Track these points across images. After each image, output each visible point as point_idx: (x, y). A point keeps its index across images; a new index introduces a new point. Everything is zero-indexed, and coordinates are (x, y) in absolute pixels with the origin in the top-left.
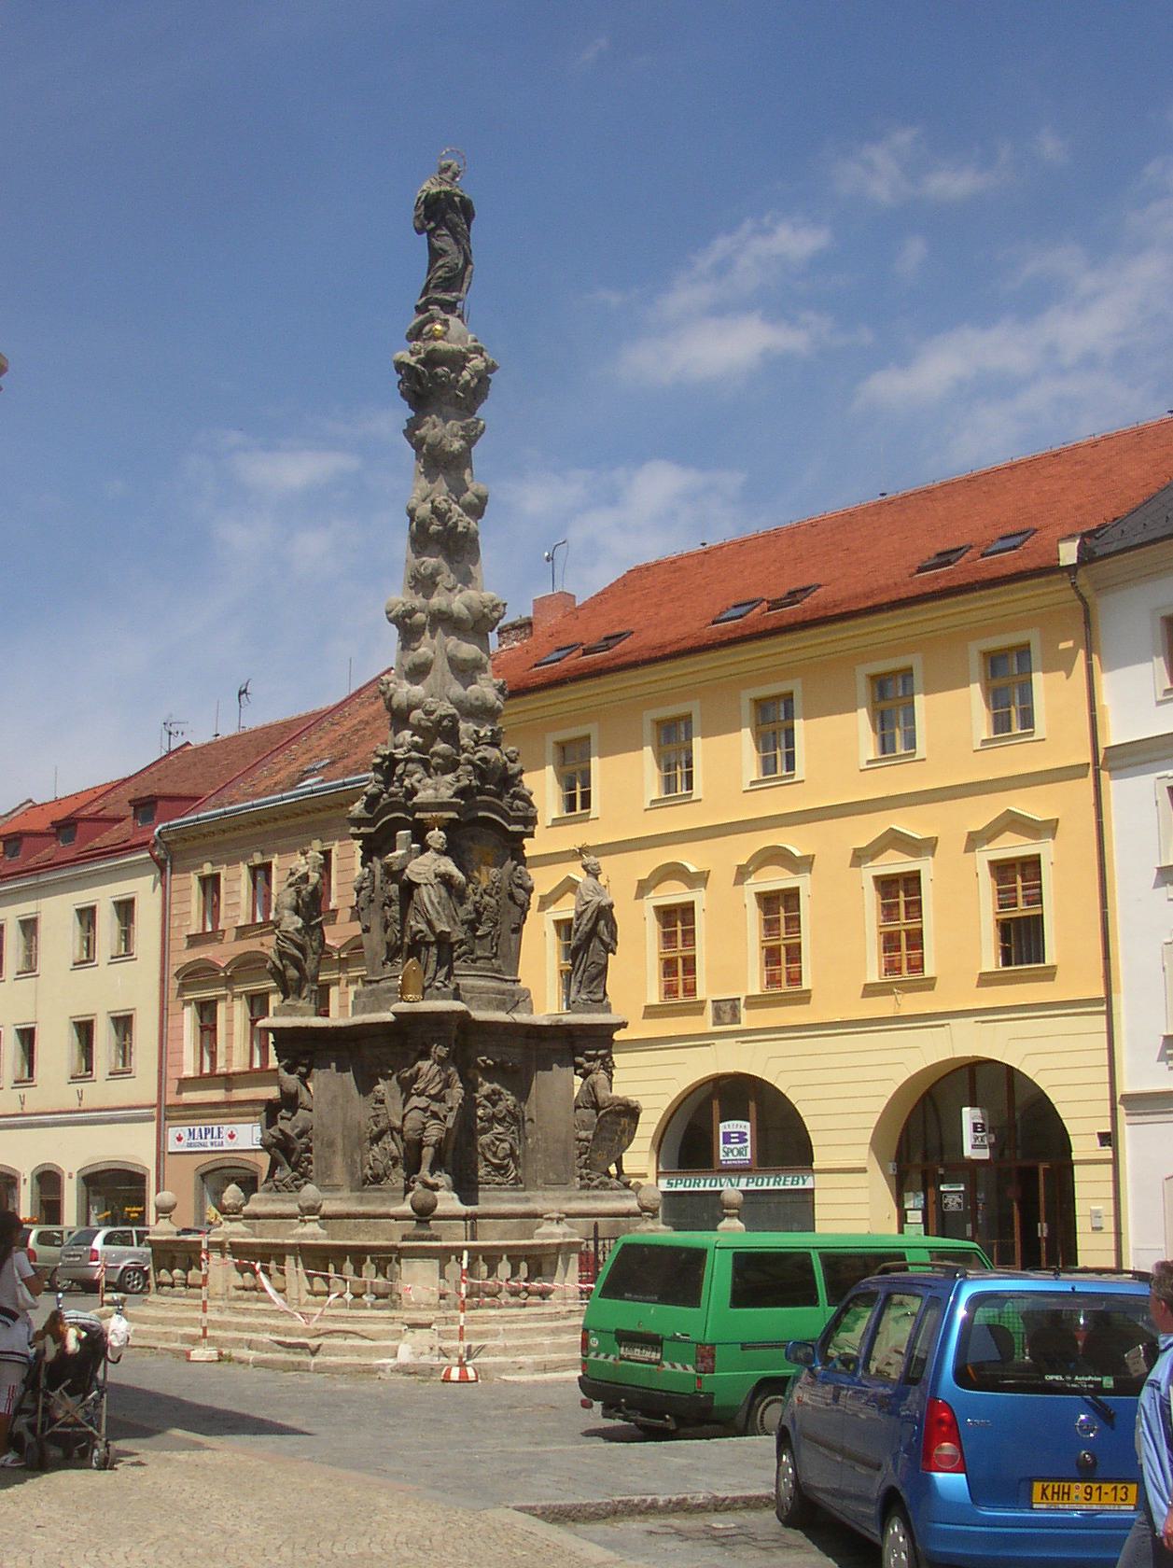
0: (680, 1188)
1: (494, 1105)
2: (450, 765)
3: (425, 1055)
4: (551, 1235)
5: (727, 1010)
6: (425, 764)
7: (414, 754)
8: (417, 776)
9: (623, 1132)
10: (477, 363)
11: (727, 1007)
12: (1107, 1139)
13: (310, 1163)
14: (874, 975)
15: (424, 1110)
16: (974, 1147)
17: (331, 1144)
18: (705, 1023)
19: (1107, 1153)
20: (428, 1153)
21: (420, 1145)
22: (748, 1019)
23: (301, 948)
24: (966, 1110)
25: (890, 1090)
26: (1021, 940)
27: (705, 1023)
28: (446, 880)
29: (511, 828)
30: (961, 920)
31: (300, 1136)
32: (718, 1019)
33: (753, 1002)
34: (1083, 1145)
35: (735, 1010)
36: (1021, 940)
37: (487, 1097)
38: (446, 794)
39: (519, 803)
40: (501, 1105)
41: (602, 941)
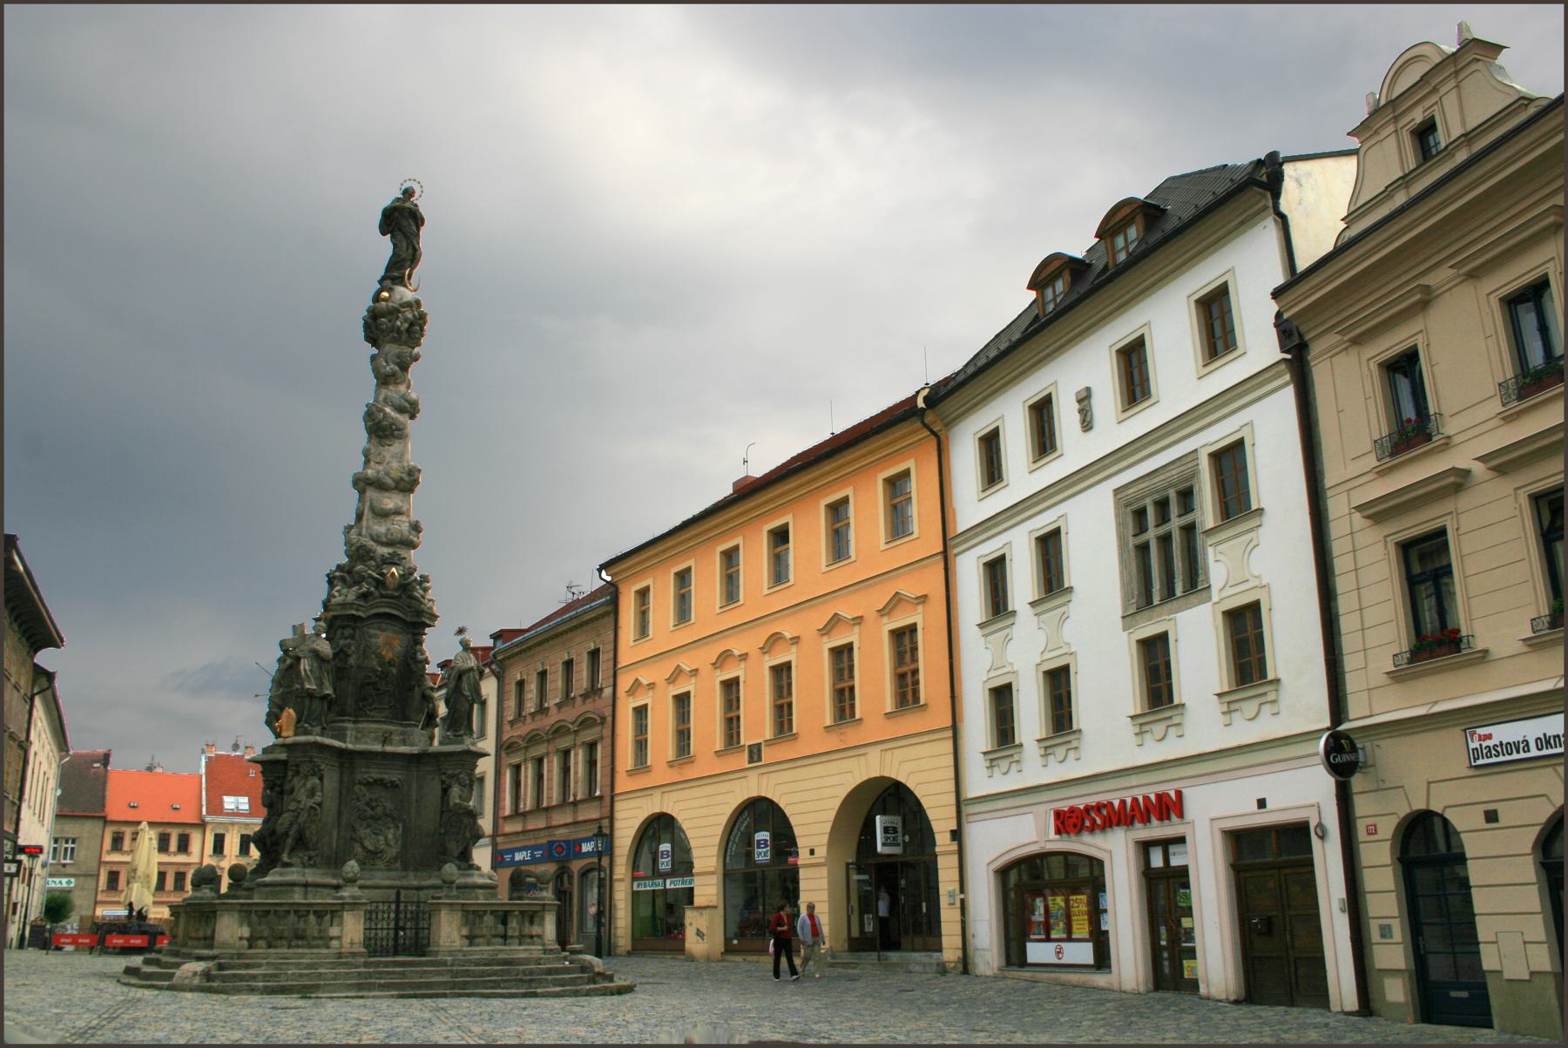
3: (298, 773)
5: (755, 753)
6: (343, 579)
12: (957, 835)
14: (828, 722)
20: (290, 841)
21: (286, 834)
22: (767, 755)
25: (836, 803)
27: (743, 760)
29: (409, 619)
32: (751, 760)
33: (769, 743)
34: (943, 841)
35: (759, 751)
36: (907, 691)
37: (368, 804)
38: (351, 597)
40: (379, 810)
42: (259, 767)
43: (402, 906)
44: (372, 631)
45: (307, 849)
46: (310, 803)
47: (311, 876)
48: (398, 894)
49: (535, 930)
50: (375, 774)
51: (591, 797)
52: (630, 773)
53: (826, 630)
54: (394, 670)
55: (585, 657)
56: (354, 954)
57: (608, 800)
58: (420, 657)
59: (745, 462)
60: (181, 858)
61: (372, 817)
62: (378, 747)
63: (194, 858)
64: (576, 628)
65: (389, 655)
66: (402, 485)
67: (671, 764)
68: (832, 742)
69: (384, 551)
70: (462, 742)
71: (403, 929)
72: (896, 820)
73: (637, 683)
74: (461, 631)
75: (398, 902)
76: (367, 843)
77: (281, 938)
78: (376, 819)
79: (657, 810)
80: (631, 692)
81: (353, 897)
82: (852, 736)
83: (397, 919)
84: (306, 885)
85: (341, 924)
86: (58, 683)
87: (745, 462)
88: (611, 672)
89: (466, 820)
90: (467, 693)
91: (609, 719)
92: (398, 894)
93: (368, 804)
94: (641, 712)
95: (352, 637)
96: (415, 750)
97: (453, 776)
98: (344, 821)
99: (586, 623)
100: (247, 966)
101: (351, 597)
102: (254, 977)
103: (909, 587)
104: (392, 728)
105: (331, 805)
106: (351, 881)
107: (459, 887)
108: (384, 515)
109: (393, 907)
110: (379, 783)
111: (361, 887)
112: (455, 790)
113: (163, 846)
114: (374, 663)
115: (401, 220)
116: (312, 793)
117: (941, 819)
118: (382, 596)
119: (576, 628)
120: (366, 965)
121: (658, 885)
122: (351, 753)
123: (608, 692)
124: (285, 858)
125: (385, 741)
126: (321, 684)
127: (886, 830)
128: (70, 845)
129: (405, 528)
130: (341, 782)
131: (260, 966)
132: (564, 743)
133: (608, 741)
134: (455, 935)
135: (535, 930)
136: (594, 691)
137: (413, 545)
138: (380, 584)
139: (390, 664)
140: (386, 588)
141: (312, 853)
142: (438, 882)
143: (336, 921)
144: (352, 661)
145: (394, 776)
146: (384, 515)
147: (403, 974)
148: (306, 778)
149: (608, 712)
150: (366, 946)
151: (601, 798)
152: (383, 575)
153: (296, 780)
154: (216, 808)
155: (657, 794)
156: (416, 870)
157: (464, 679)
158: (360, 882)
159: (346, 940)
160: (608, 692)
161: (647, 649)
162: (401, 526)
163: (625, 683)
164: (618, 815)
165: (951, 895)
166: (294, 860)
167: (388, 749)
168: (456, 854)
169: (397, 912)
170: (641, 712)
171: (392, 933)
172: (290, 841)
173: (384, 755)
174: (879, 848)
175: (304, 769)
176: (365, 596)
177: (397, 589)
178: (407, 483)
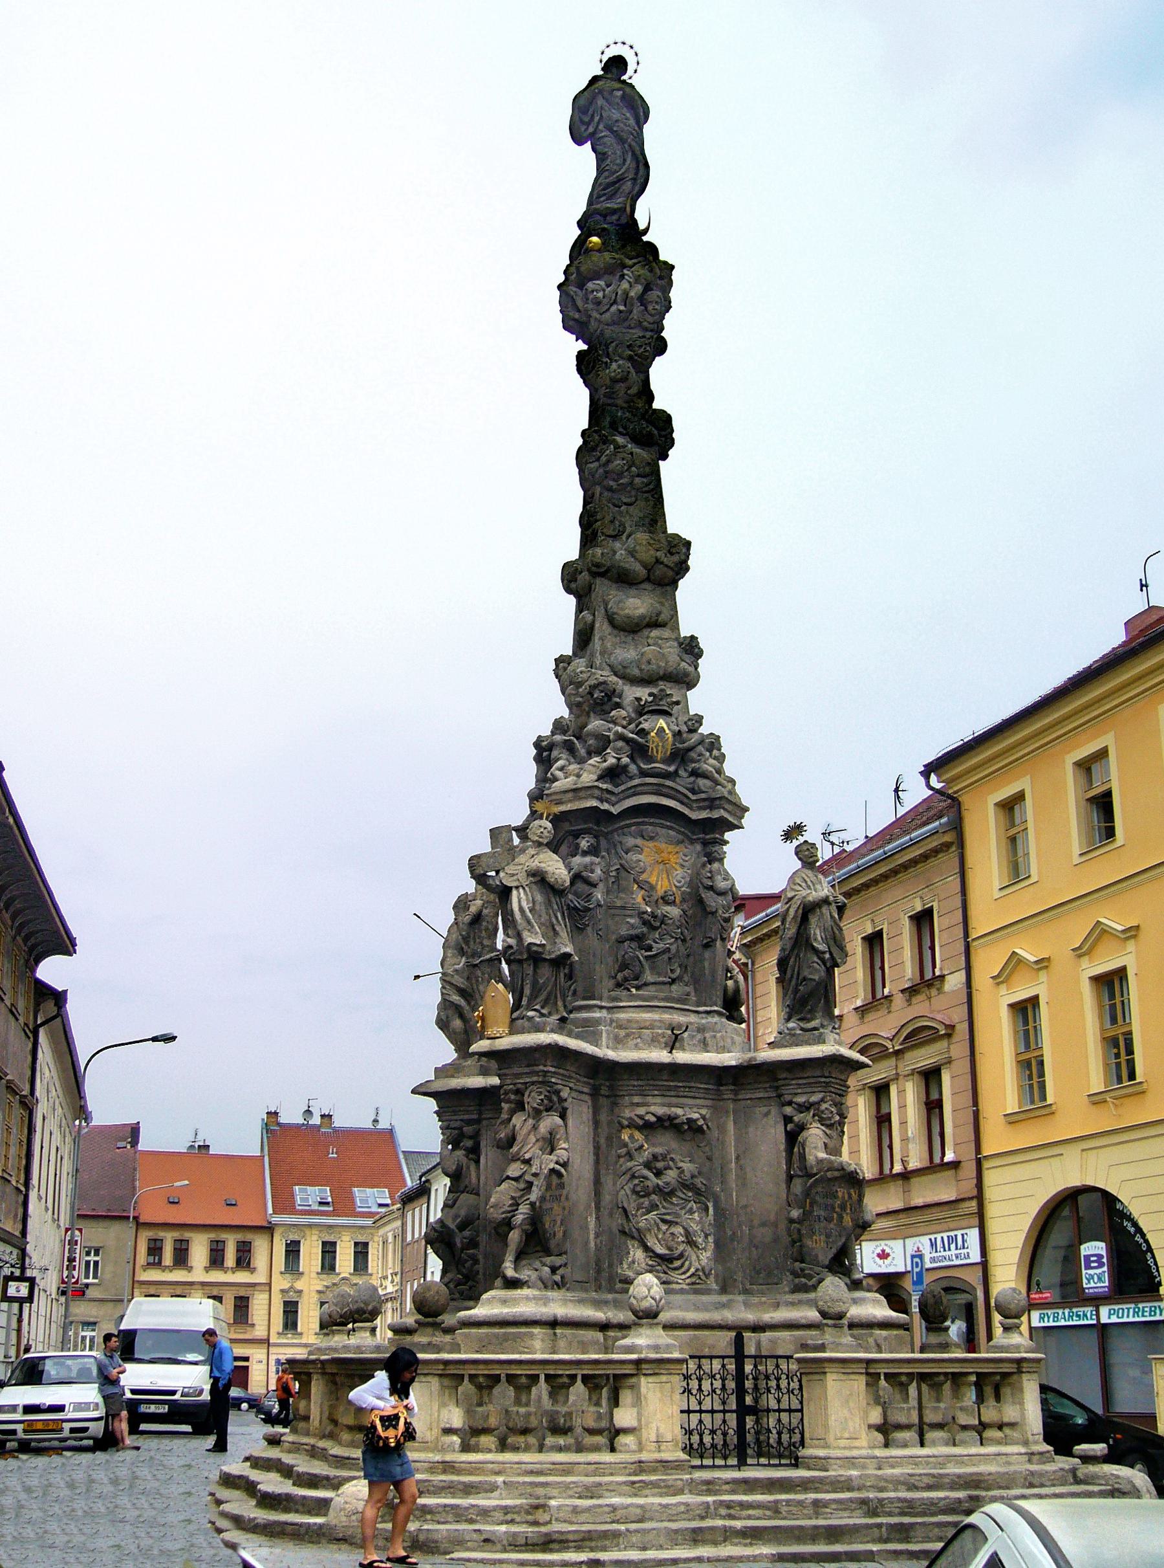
1: (658, 1174)
2: (602, 745)
3: (520, 1106)
4: (630, 1349)
6: (570, 748)
7: (558, 738)
8: (560, 763)
9: (843, 1207)
13: (476, 1262)
15: (516, 1179)
20: (514, 1236)
21: (507, 1224)
23: (462, 992)
28: (540, 879)
29: (694, 816)
31: (462, 1227)
37: (648, 1165)
38: (588, 778)
39: (702, 782)
40: (671, 1176)
41: (816, 951)
42: (432, 1104)
43: (748, 1368)
44: (630, 841)
45: (548, 1253)
46: (549, 1162)
47: (559, 1306)
48: (739, 1342)
49: (1010, 1413)
50: (657, 1108)
51: (935, 1167)
54: (674, 912)
55: (906, 927)
56: (665, 1465)
57: (969, 1170)
58: (722, 885)
59: (1143, 586)
60: (242, 1277)
61: (658, 1190)
62: (661, 1056)
63: (260, 1277)
64: (885, 877)
65: (662, 886)
66: (659, 571)
67: (1096, 1100)
69: (633, 693)
70: (821, 1040)
71: (754, 1410)
73: (1014, 962)
74: (791, 833)
75: (740, 1356)
76: (651, 1242)
77: (525, 1431)
78: (667, 1194)
79: (1075, 1182)
80: (999, 979)
81: (656, 1348)
83: (741, 1392)
84: (554, 1323)
85: (638, 1402)
86: (69, 1006)
87: (1143, 586)
88: (961, 947)
89: (841, 1192)
90: (822, 947)
91: (962, 1028)
92: (739, 1342)
93: (648, 1165)
94: (1025, 1010)
95: (593, 851)
96: (729, 1059)
97: (804, 1108)
98: (607, 1198)
99: (905, 867)
100: (468, 1489)
101: (588, 778)
102: (485, 1513)
104: (681, 1019)
105: (582, 1168)
106: (649, 1316)
107: (852, 1326)
108: (632, 628)
109: (732, 1367)
110: (666, 1124)
111: (667, 1327)
112: (815, 1135)
113: (216, 1259)
114: (639, 897)
116: (550, 1144)
118: (644, 774)
119: (885, 877)
120: (694, 1487)
121: (1085, 1316)
122: (613, 1068)
123: (955, 981)
124: (510, 1272)
125: (674, 1043)
126: (551, 931)
128: (92, 1258)
129: (672, 653)
130: (596, 1123)
131: (493, 1488)
132: (877, 1073)
133: (963, 1066)
134: (857, 1424)
135: (1010, 1413)
136: (926, 983)
137: (688, 681)
138: (639, 750)
139: (666, 900)
140: (651, 759)
141: (558, 1261)
142: (813, 1315)
143: (626, 1396)
144: (599, 895)
145: (691, 1111)
146: (632, 628)
147: (775, 1509)
148: (537, 1114)
149: (958, 1016)
150: (689, 1449)
151: (955, 1165)
152: (643, 733)
153: (518, 1120)
154: (284, 1203)
155: (1072, 1153)
156: (746, 1292)
157: (813, 920)
158: (664, 1317)
159: (650, 1434)
160: (955, 981)
161: (1025, 903)
162: (656, 651)
163: (988, 962)
164: (990, 1193)
166: (525, 1274)
167: (682, 1057)
168: (825, 1257)
169: (740, 1376)
170: (1025, 1010)
171: (732, 1419)
172: (514, 1236)
173: (675, 1070)
175: (533, 1099)
176: (613, 774)
177: (669, 760)
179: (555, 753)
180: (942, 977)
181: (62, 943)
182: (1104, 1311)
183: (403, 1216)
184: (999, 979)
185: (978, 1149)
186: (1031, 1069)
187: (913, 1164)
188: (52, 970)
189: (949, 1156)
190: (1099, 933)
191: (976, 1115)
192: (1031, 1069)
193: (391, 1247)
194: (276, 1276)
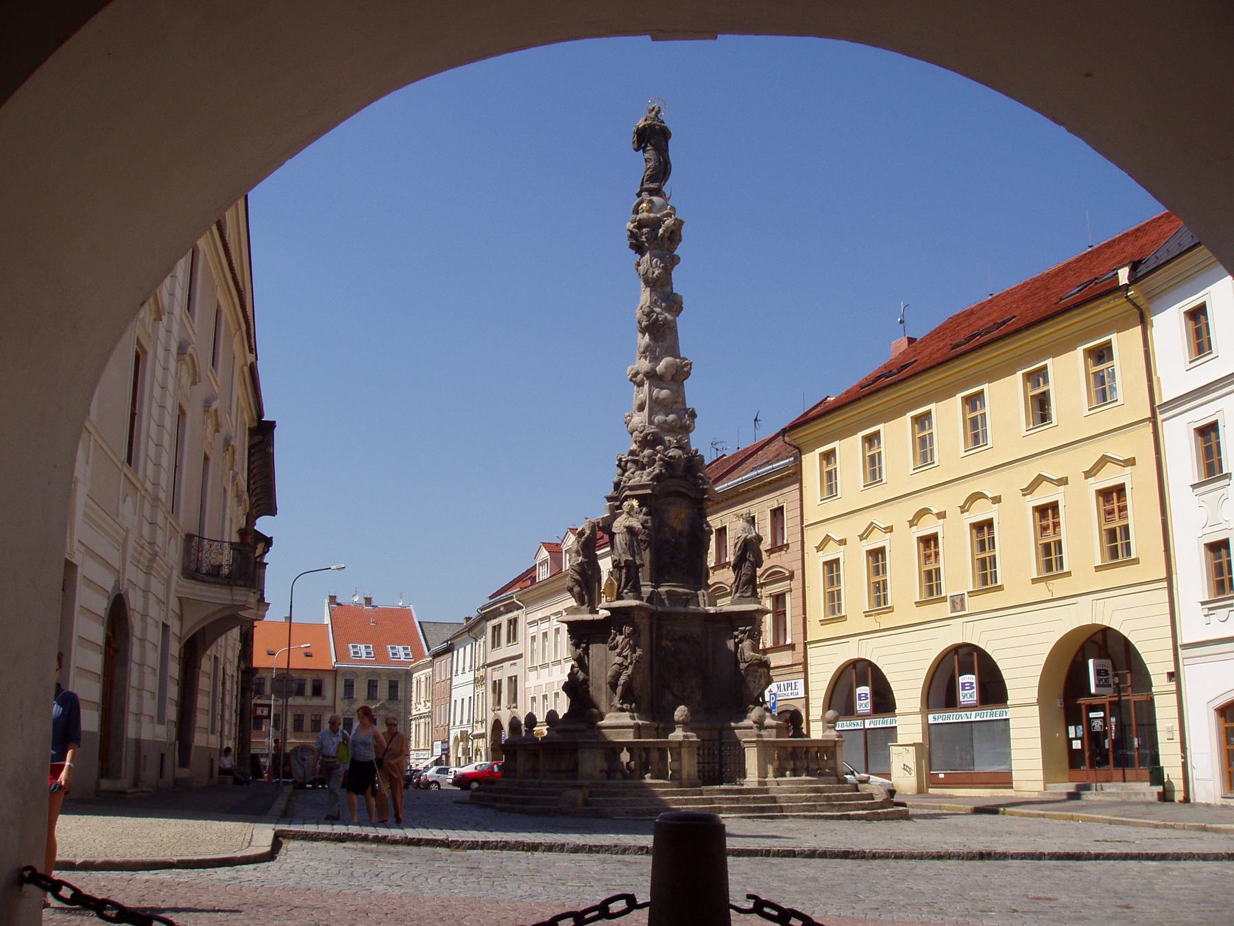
0: (940, 721)
5: (958, 603)
10: (669, 222)
11: (958, 601)
12: (1174, 676)
16: (1097, 686)
17: (599, 689)
18: (944, 609)
19: (1173, 686)
22: (971, 604)
24: (1091, 662)
26: (1116, 545)
28: (630, 530)
30: (1081, 532)
32: (954, 609)
34: (1159, 682)
35: (962, 600)
36: (1116, 545)
52: (823, 622)
53: (1029, 490)
57: (799, 648)
60: (316, 701)
63: (328, 701)
67: (867, 614)
68: (1041, 591)
72: (1107, 664)
73: (827, 539)
80: (819, 549)
82: (1059, 587)
91: (798, 574)
94: (832, 566)
103: (1117, 448)
115: (653, 137)
117: (1157, 662)
121: (857, 724)
123: (795, 548)
127: (1098, 673)
151: (792, 647)
161: (834, 507)
165: (1170, 731)
170: (832, 566)
174: (1093, 690)
178: (679, 374)
179: (629, 465)
180: (787, 545)
181: (271, 510)
182: (867, 722)
183: (432, 666)
184: (819, 549)
185: (805, 638)
186: (833, 599)
187: (768, 646)
188: (264, 525)
189: (789, 641)
190: (871, 527)
191: (805, 619)
192: (833, 599)
193: (423, 685)
194: (338, 701)
